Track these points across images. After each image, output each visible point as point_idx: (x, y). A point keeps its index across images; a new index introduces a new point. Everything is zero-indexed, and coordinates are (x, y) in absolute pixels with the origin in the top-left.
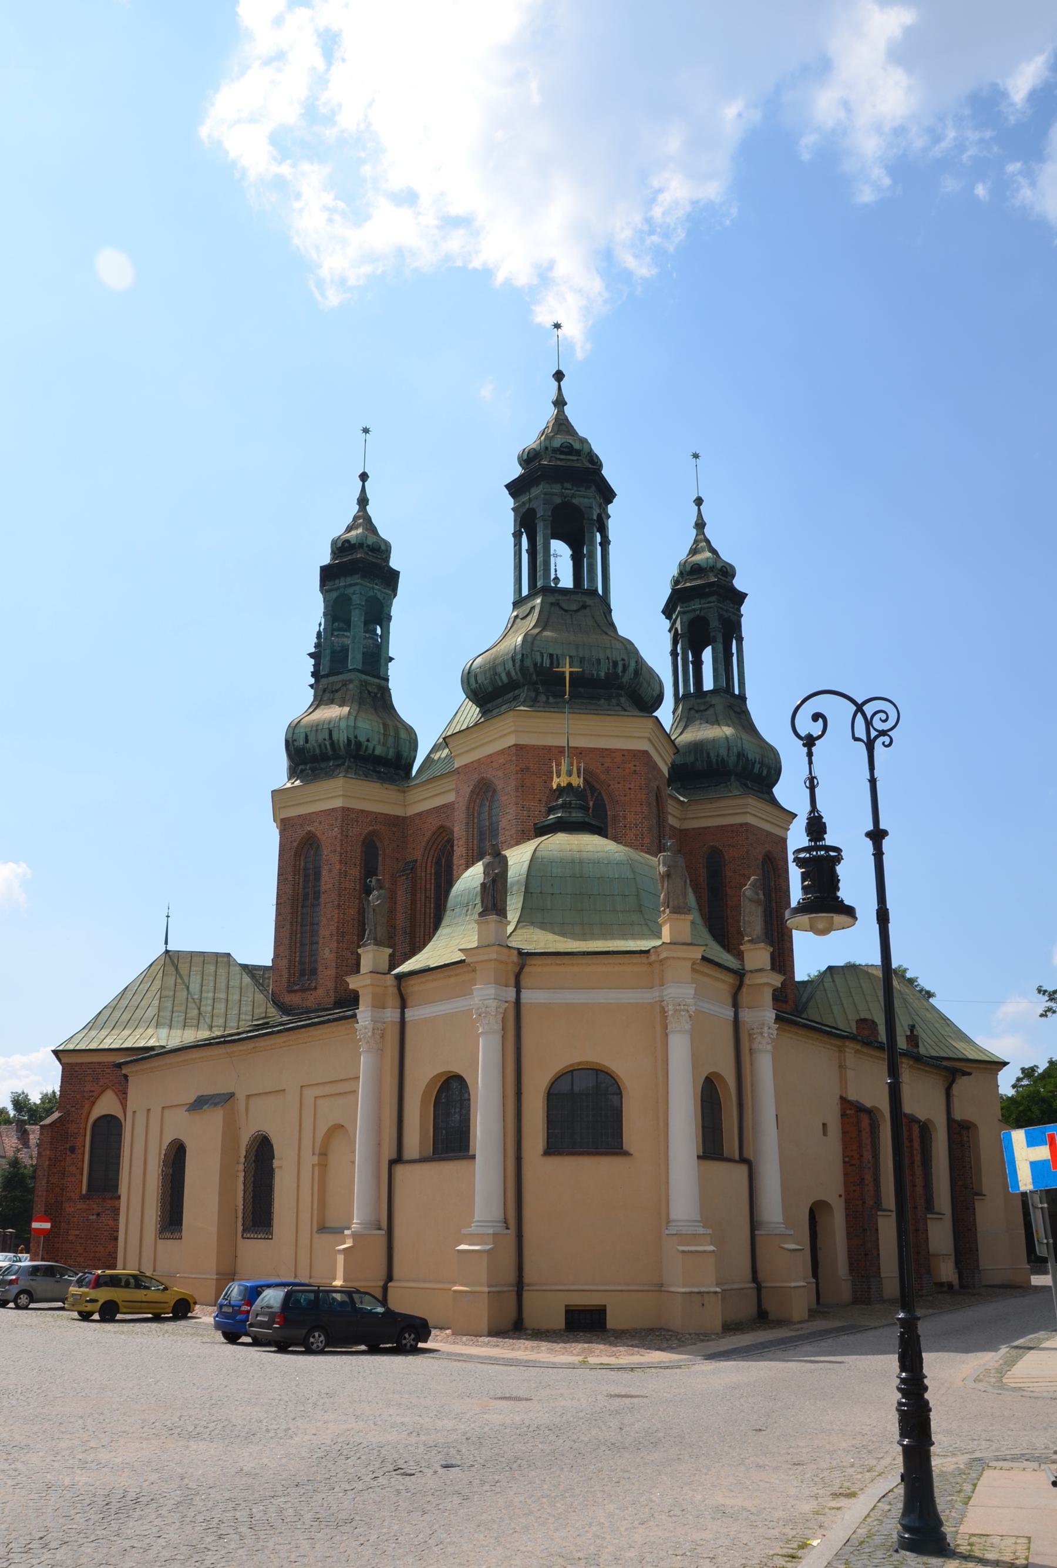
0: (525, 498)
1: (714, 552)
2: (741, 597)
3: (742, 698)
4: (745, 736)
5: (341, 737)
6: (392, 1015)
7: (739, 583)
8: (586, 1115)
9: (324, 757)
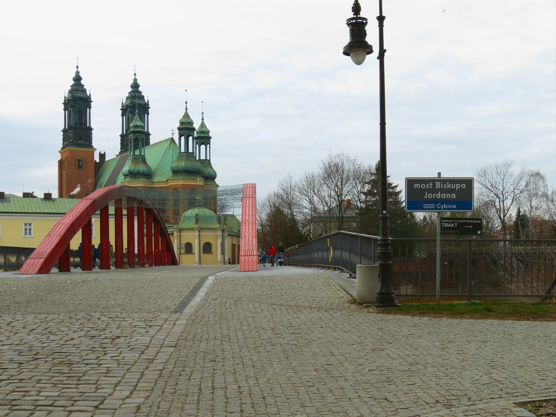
0: (181, 132)
1: (206, 126)
2: (210, 138)
3: (210, 160)
4: (211, 170)
5: (141, 171)
6: (179, 234)
7: (210, 134)
8: (207, 248)
9: (137, 174)
